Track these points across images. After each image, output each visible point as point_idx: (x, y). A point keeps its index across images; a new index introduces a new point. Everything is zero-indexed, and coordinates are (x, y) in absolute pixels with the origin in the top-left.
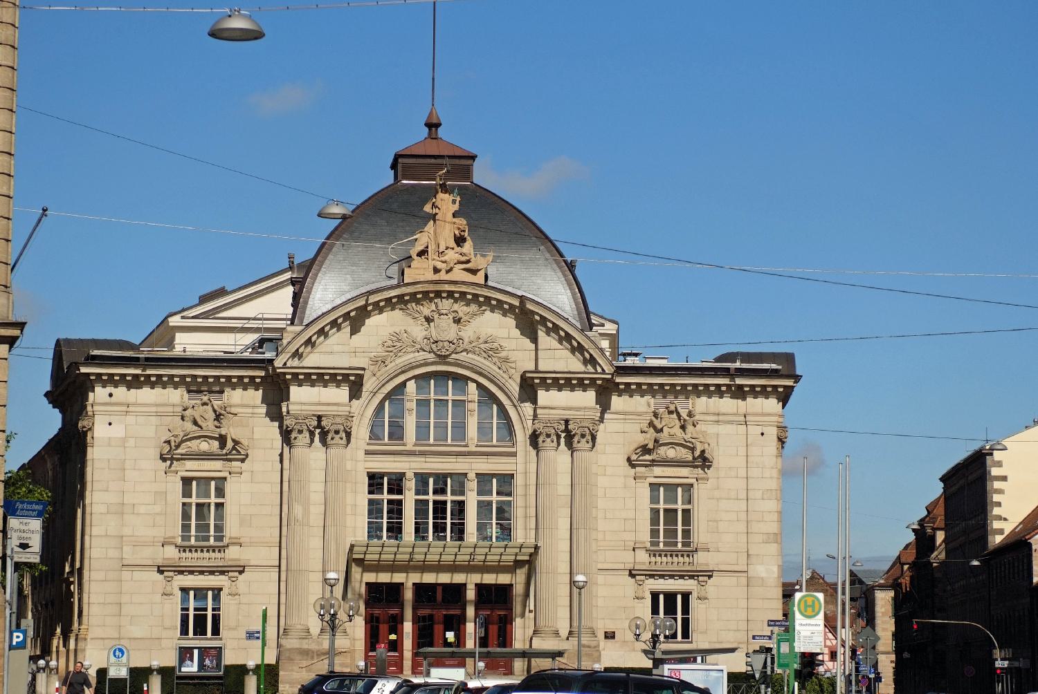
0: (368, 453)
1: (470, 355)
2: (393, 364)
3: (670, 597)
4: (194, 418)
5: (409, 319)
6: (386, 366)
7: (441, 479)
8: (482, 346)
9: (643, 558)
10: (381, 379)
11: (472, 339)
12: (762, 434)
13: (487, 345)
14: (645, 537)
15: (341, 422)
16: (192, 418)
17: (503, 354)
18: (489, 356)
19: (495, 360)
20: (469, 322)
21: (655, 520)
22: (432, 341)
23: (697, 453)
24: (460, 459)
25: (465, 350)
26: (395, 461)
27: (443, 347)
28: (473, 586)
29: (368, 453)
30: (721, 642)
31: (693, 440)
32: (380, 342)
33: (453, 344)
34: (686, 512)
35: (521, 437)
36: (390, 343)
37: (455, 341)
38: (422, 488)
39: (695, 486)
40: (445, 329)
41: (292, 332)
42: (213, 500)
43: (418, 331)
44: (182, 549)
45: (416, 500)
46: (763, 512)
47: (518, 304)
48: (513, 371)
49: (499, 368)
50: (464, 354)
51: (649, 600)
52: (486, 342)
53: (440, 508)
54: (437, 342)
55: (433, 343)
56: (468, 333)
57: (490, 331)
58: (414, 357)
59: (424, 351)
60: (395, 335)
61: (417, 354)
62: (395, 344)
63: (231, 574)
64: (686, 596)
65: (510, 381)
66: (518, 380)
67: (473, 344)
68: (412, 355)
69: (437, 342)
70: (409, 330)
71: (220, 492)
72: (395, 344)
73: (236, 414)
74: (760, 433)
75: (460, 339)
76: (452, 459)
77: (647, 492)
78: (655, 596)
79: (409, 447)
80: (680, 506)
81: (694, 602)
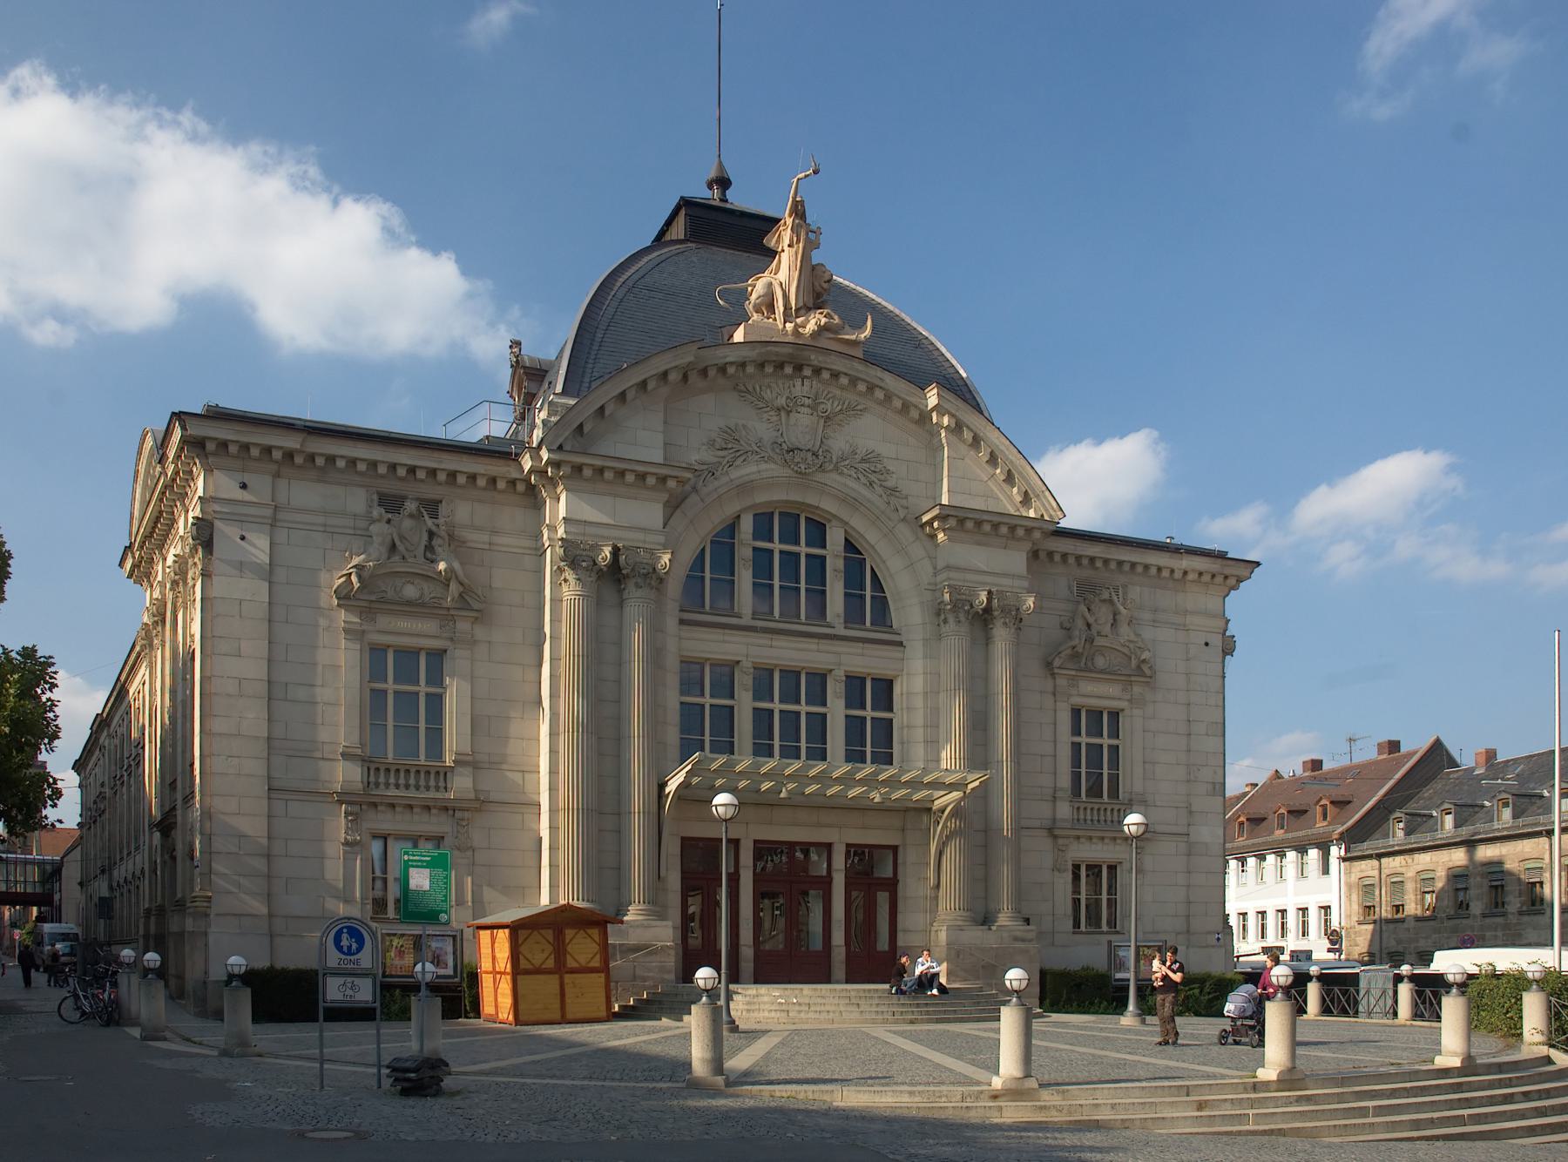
0: (682, 622)
2: (725, 479)
3: (1094, 869)
4: (393, 541)
7: (791, 676)
9: (1064, 810)
12: (1207, 644)
13: (867, 465)
14: (1065, 781)
15: (650, 561)
16: (388, 540)
17: (890, 484)
19: (879, 490)
21: (1076, 762)
23: (1134, 663)
24: (825, 645)
26: (724, 642)
28: (843, 849)
29: (682, 622)
30: (1158, 933)
31: (1131, 646)
33: (817, 456)
34: (1114, 750)
35: (909, 613)
36: (720, 443)
38: (762, 689)
39: (1127, 712)
40: (801, 429)
41: (563, 405)
42: (423, 688)
43: (761, 428)
44: (373, 767)
45: (755, 709)
46: (1207, 753)
50: (834, 476)
51: (1069, 876)
52: (863, 460)
53: (791, 719)
54: (792, 451)
55: (788, 452)
56: (839, 443)
58: (759, 472)
59: (776, 463)
60: (729, 430)
61: (764, 466)
62: (730, 446)
63: (458, 814)
64: (1112, 868)
67: (846, 463)
68: (754, 468)
69: (792, 451)
71: (436, 678)
72: (732, 445)
73: (464, 542)
74: (1203, 643)
75: (827, 451)
76: (812, 644)
77: (1065, 719)
78: (1076, 867)
79: (747, 620)
80: (1106, 741)
81: (1128, 881)
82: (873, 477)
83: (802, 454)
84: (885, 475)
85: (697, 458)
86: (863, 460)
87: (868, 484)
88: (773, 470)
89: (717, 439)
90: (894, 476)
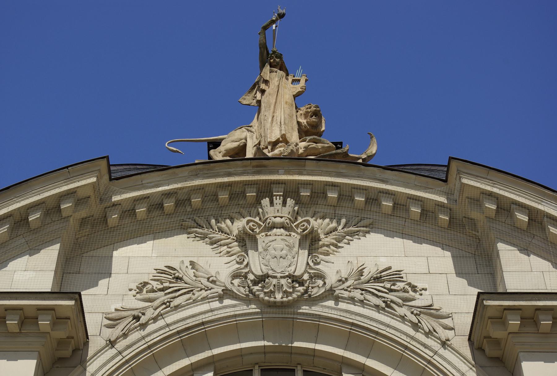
1: (342, 305)
2: (161, 323)
5: (203, 247)
6: (143, 326)
10: (128, 354)
11: (344, 275)
17: (422, 301)
18: (388, 306)
20: (336, 246)
22: (251, 277)
25: (330, 294)
27: (280, 287)
32: (134, 286)
33: (301, 284)
36: (156, 285)
37: (306, 277)
47: (443, 199)
48: (450, 334)
49: (416, 326)
55: (255, 283)
57: (383, 263)
59: (234, 296)
61: (216, 304)
65: (446, 353)
66: (467, 352)
68: (205, 307)
70: (201, 262)
82: (391, 296)
83: (274, 281)
84: (411, 293)
85: (119, 306)
86: (377, 279)
87: (383, 305)
88: (234, 306)
90: (427, 293)
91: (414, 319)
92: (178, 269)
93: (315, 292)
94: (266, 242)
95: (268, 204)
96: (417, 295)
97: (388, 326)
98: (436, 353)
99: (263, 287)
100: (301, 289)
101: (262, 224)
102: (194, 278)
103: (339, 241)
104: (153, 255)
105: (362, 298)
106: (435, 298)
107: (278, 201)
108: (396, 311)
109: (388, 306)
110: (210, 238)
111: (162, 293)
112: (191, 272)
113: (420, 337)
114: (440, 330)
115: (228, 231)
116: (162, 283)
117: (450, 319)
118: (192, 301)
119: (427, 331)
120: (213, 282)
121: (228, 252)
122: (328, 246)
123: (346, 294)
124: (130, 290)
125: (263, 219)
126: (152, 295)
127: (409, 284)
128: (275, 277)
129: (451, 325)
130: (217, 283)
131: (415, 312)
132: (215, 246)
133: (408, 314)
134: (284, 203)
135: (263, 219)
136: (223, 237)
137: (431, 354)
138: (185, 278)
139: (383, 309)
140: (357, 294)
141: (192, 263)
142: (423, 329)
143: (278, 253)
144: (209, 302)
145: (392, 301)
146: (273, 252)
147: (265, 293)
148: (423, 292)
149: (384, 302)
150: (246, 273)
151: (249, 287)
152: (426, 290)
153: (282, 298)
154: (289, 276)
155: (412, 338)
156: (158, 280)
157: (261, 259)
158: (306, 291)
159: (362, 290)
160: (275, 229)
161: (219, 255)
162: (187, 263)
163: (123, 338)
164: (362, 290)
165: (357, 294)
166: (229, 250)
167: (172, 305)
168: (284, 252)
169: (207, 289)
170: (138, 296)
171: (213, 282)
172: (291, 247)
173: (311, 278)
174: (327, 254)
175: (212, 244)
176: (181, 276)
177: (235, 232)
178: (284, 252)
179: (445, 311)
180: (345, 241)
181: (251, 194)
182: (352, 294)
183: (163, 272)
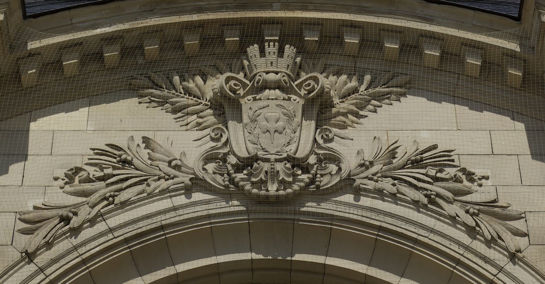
1: (365, 201)
2: (100, 227)
6: (75, 231)
8: (399, 173)
11: (368, 156)
18: (432, 202)
22: (232, 160)
32: (61, 173)
33: (306, 170)
36: (93, 172)
37: (312, 160)
47: (514, 46)
48: (522, 242)
49: (472, 232)
55: (238, 169)
61: (181, 200)
62: (109, 171)
68: (166, 204)
70: (159, 138)
82: (436, 188)
83: (266, 166)
84: (466, 183)
85: (39, 203)
86: (417, 163)
87: (425, 200)
89: (85, 167)
90: (489, 182)
91: (470, 221)
92: (126, 148)
93: (326, 182)
94: (254, 109)
95: (258, 54)
96: (474, 187)
97: (432, 231)
98: (501, 269)
99: (250, 175)
100: (305, 177)
101: (248, 82)
102: (149, 162)
103: (362, 108)
104: (89, 128)
105: (394, 190)
106: (500, 190)
107: (271, 49)
108: (443, 209)
109: (432, 202)
110: (172, 104)
111: (103, 184)
112: (144, 153)
113: (479, 246)
114: (507, 236)
115: (199, 94)
116: (102, 169)
117: (523, 220)
118: (145, 194)
119: (489, 237)
120: (177, 167)
121: (199, 124)
122: (345, 115)
123: (371, 185)
124: (56, 179)
125: (250, 75)
126: (87, 186)
127: (463, 170)
128: (267, 160)
129: (524, 230)
130: (183, 169)
131: (471, 210)
132: (180, 114)
133: (462, 213)
134: (281, 53)
135: (250, 75)
136: (191, 102)
137: (495, 271)
138: (135, 161)
139: (425, 206)
140: (387, 185)
141: (146, 140)
142: (483, 236)
143: (272, 126)
144: (171, 197)
145: (438, 195)
146: (265, 123)
147: (253, 183)
148: (483, 181)
149: (426, 196)
150: (226, 154)
151: (229, 174)
152: (487, 178)
153: (277, 190)
154: (289, 159)
155: (467, 248)
156: (95, 165)
157: (247, 134)
158: (312, 181)
159: (395, 179)
160: (267, 90)
161: (185, 128)
162: (139, 140)
163: (45, 248)
164: (395, 179)
165: (387, 185)
166: (200, 120)
167: (117, 200)
168: (281, 124)
169: (169, 177)
170: (68, 188)
171: (177, 167)
172: (290, 117)
173: (320, 161)
174: (344, 127)
175: (174, 112)
176: (129, 158)
177: (209, 95)
178: (281, 124)
179: (515, 209)
180: (370, 107)
181: (232, 39)
182: (379, 185)
183: (103, 153)
